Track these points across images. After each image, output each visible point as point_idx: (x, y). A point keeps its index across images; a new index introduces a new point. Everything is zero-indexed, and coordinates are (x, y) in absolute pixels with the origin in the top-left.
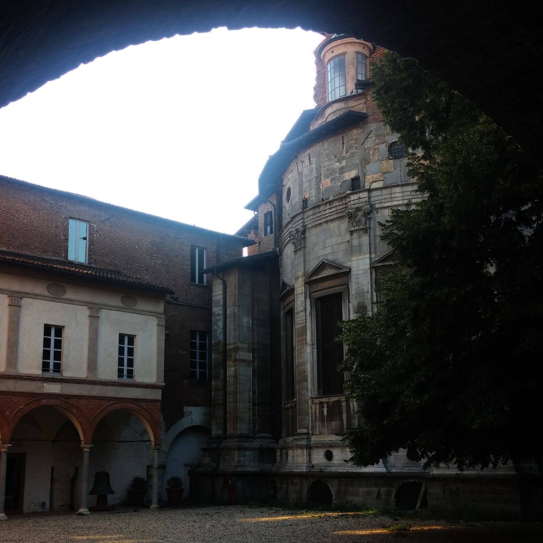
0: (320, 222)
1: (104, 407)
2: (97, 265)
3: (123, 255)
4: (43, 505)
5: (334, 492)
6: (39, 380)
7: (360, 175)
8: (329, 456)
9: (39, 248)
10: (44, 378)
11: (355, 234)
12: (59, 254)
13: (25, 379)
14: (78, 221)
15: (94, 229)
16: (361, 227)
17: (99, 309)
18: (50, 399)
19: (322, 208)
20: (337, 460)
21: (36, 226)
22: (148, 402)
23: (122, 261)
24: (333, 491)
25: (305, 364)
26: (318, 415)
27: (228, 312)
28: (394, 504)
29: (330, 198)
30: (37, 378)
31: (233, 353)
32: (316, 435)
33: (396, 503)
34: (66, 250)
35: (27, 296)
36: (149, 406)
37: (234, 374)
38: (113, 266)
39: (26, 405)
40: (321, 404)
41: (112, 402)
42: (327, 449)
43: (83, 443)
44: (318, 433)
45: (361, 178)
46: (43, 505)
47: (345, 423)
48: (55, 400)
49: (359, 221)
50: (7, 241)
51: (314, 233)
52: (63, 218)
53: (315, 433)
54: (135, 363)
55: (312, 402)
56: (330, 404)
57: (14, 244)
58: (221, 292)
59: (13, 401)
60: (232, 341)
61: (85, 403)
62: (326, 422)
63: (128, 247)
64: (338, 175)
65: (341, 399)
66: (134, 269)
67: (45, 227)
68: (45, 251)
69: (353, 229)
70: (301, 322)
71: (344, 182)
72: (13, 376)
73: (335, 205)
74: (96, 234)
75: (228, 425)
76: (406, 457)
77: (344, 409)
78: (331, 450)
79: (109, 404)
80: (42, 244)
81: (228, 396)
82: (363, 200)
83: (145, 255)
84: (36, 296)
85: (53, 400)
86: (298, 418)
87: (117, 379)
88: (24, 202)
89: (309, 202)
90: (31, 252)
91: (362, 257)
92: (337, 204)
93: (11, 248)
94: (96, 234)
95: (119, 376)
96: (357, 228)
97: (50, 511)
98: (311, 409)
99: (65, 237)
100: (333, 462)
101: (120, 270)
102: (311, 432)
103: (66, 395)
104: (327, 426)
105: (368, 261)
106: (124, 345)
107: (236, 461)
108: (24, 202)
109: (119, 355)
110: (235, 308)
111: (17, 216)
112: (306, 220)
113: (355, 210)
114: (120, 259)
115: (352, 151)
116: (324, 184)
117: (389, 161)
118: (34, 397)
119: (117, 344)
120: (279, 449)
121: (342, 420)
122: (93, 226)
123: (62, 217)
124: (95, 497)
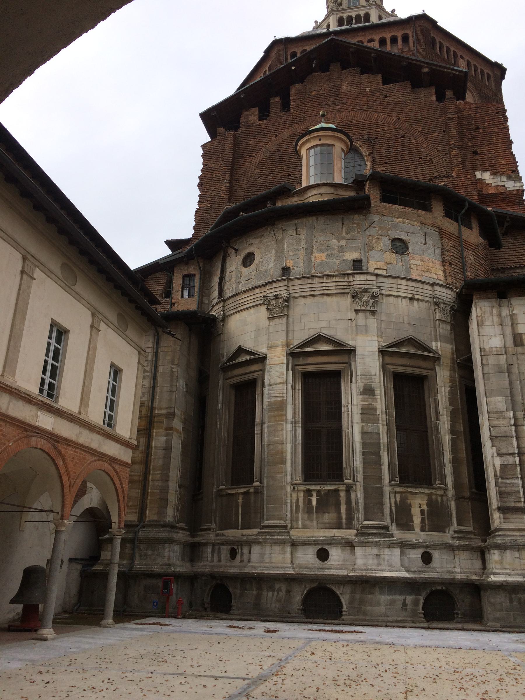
0: (312, 293)
5: (345, 601)
7: (363, 258)
8: (323, 555)
10: (42, 401)
11: (360, 314)
16: (368, 308)
18: (41, 437)
19: (316, 280)
20: (335, 561)
24: (344, 600)
25: (283, 443)
26: (301, 504)
27: (161, 369)
28: (422, 616)
29: (325, 273)
30: (35, 401)
31: (165, 420)
32: (298, 528)
33: (424, 614)
35: (42, 267)
37: (164, 445)
39: (15, 442)
40: (309, 493)
42: (320, 547)
44: (300, 526)
45: (364, 261)
47: (344, 516)
49: (366, 302)
51: (303, 303)
53: (295, 526)
55: (294, 488)
56: (323, 493)
58: (150, 345)
60: (164, 405)
62: (315, 514)
64: (336, 252)
65: (340, 489)
69: (359, 308)
70: (278, 395)
71: (344, 260)
72: (10, 387)
73: (334, 280)
75: (148, 509)
76: (420, 560)
77: (343, 500)
78: (327, 549)
81: (151, 472)
82: (371, 283)
85: (43, 440)
86: (267, 507)
89: (293, 271)
91: (369, 338)
92: (338, 280)
96: (363, 308)
98: (291, 497)
100: (329, 563)
102: (289, 525)
104: (316, 518)
105: (376, 344)
107: (166, 558)
110: (174, 366)
112: (290, 288)
113: (361, 290)
115: (353, 233)
116: (317, 258)
117: (392, 253)
118: (26, 430)
120: (210, 544)
121: (339, 512)
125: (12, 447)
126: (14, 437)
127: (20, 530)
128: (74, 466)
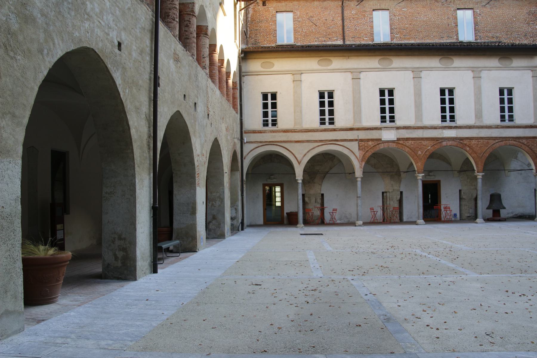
1: (491, 145)
2: (482, 40)
3: (503, 28)
4: (455, 215)
6: (439, 128)
9: (436, 36)
10: (443, 126)
12: (452, 37)
13: (429, 128)
14: (464, 10)
15: (477, 14)
17: (481, 71)
18: (448, 141)
21: (434, 21)
22: (528, 139)
23: (502, 33)
34: (457, 33)
36: (529, 142)
38: (495, 39)
39: (432, 147)
41: (497, 141)
43: (476, 172)
46: (455, 215)
48: (452, 142)
50: (414, 35)
52: (452, 11)
54: (515, 109)
57: (419, 36)
59: (422, 144)
61: (476, 142)
63: (506, 21)
66: (514, 37)
67: (440, 20)
68: (442, 37)
74: (479, 16)
79: (495, 142)
80: (439, 33)
83: (523, 24)
84: (431, 69)
85: (451, 142)
87: (500, 123)
88: (423, 6)
90: (431, 40)
93: (417, 40)
94: (479, 16)
95: (501, 121)
97: (460, 220)
99: (455, 24)
101: (501, 40)
103: (460, 138)
106: (504, 96)
108: (423, 6)
109: (500, 104)
111: (419, 17)
114: (501, 32)
119: (498, 97)
122: (476, 11)
123: (451, 10)
124: (490, 212)
125: (431, 149)
126: (431, 144)
127: (505, 176)
128: (479, 148)
